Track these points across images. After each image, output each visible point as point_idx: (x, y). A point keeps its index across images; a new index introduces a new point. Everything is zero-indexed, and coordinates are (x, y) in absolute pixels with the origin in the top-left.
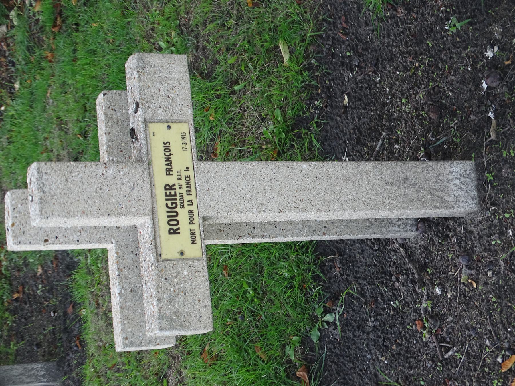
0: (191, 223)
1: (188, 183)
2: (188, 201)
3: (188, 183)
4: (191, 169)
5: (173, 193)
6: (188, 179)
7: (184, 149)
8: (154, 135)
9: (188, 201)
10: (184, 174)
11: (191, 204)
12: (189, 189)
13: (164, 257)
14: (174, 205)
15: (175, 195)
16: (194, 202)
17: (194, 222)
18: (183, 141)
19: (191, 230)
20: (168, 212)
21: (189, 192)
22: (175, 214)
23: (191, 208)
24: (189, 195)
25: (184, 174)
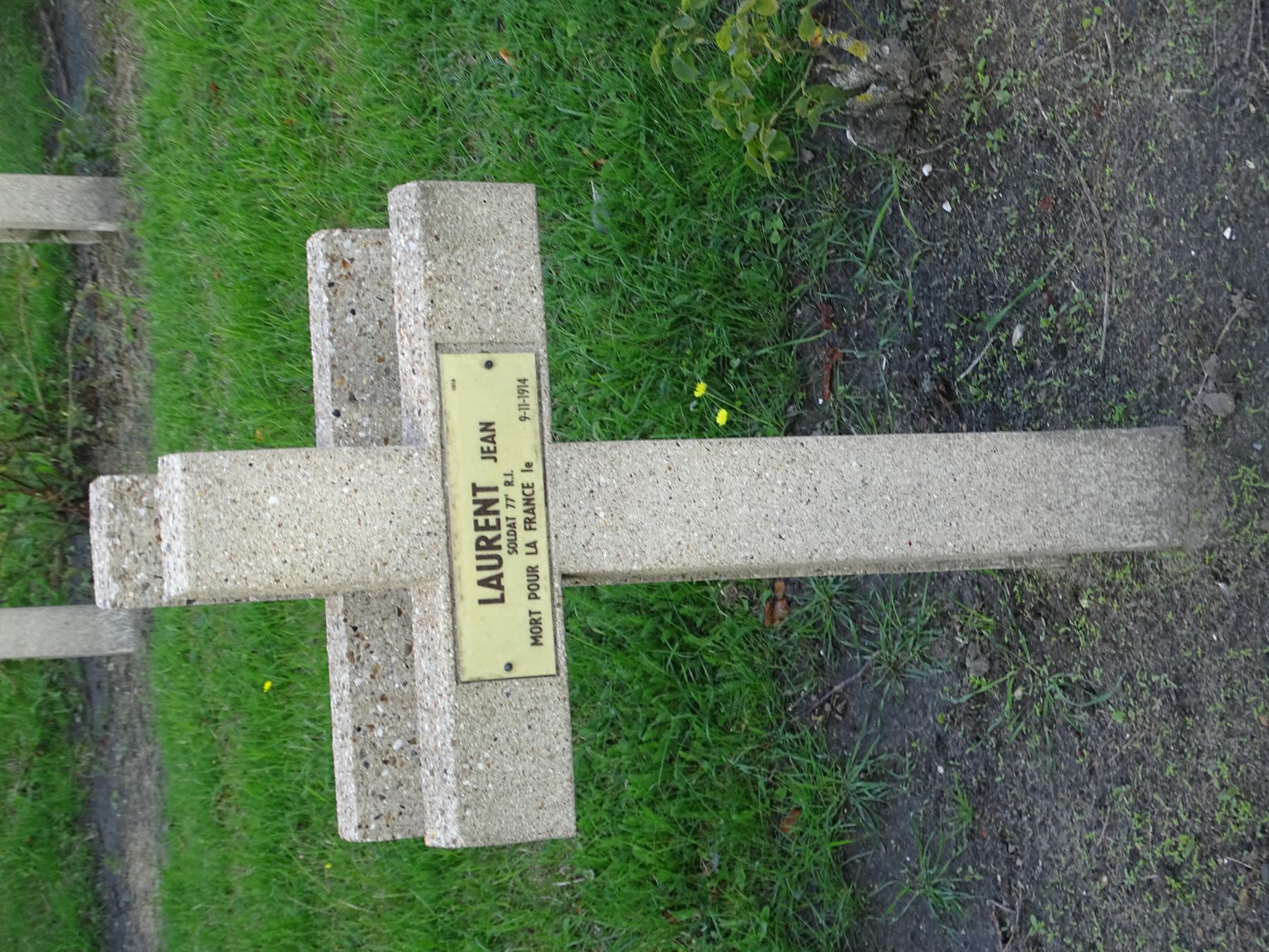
0: (533, 596)
1: (528, 501)
2: (528, 545)
3: (528, 501)
4: (537, 467)
6: (528, 491)
8: (454, 387)
9: (528, 545)
10: (520, 478)
11: (533, 550)
12: (531, 516)
15: (498, 527)
16: (542, 545)
17: (538, 593)
18: (521, 401)
19: (531, 613)
20: (479, 568)
22: (495, 562)
23: (532, 561)
24: (531, 529)
25: (520, 478)
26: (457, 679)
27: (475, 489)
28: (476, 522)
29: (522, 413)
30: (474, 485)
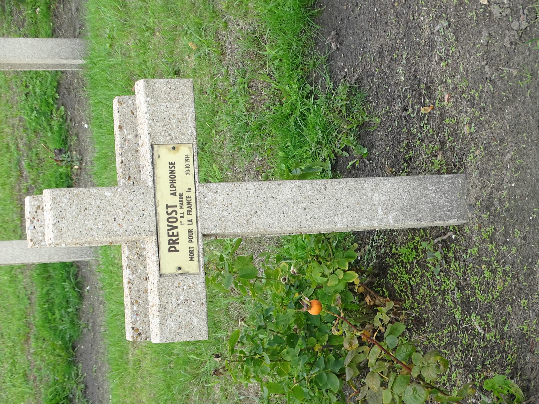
0: (190, 241)
1: (189, 203)
2: (189, 221)
3: (189, 203)
4: (193, 190)
6: (189, 199)
7: (188, 172)
9: (189, 221)
12: (190, 209)
13: (163, 272)
17: (193, 240)
18: (187, 163)
19: (189, 248)
21: (189, 213)
23: (190, 227)
24: (190, 214)
27: (168, 207)
29: (187, 169)
30: (167, 205)
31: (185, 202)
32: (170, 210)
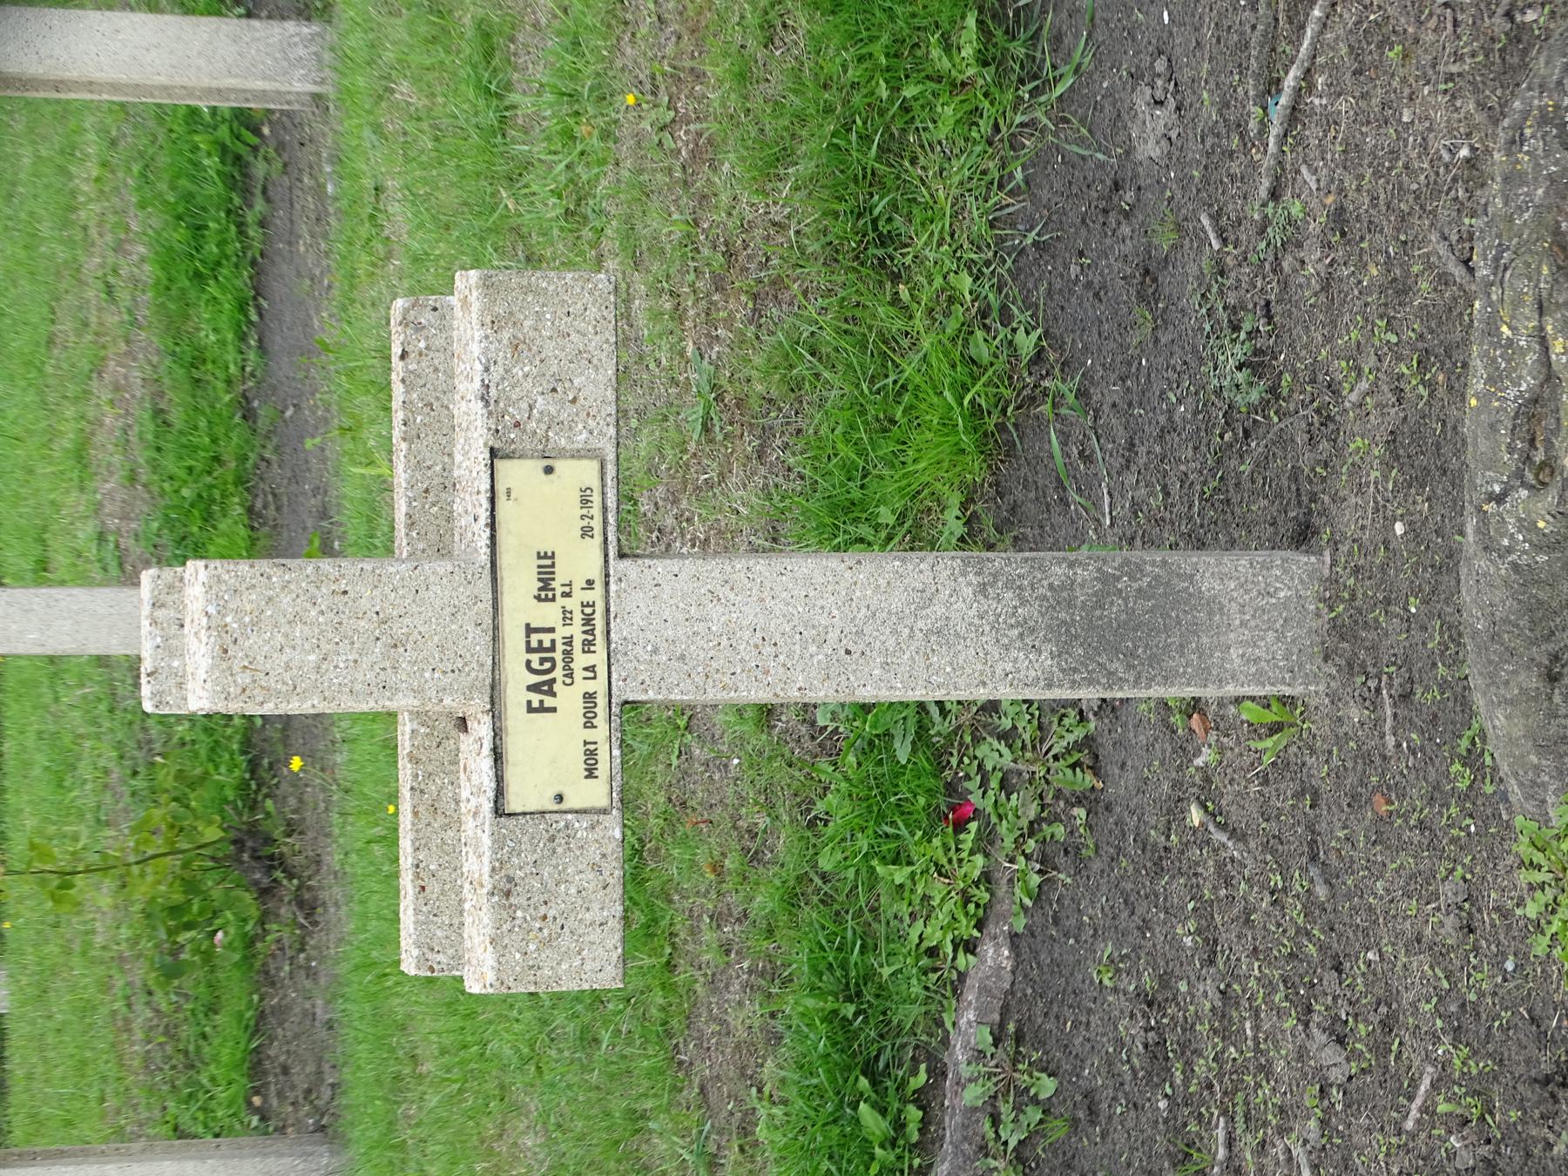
0: (589, 725)
1: (588, 620)
2: (586, 669)
3: (588, 620)
4: (599, 586)
5: (547, 644)
6: (588, 610)
9: (586, 669)
10: (580, 596)
14: (547, 665)
15: (552, 649)
18: (584, 511)
19: (586, 743)
21: (588, 646)
23: (591, 686)
24: (589, 652)
25: (580, 596)
26: (499, 811)
28: (528, 663)
31: (578, 618)
32: (535, 638)
